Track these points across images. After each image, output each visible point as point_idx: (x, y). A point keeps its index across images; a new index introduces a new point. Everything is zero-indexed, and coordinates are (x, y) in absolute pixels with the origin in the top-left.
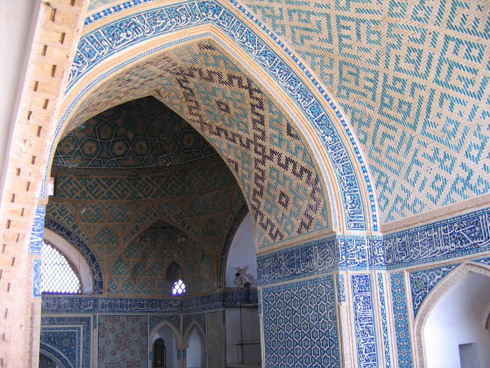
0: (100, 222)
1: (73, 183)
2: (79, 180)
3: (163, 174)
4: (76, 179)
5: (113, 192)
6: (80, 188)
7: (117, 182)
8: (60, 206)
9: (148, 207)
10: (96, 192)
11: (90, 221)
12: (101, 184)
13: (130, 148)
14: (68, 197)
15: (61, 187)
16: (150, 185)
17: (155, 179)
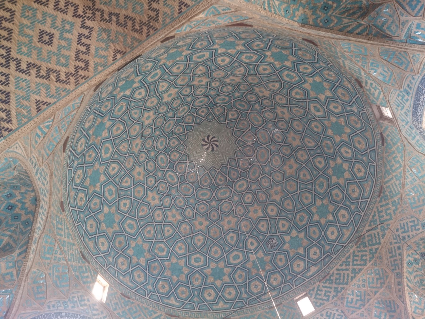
0: (368, 302)
1: (323, 289)
2: (326, 283)
3: (373, 214)
4: (323, 284)
5: (355, 267)
6: (331, 288)
7: (351, 256)
8: (325, 315)
9: (388, 249)
10: (344, 280)
11: (360, 309)
12: (342, 270)
13: (338, 225)
14: (325, 302)
15: (315, 298)
16: (373, 232)
17: (372, 223)
